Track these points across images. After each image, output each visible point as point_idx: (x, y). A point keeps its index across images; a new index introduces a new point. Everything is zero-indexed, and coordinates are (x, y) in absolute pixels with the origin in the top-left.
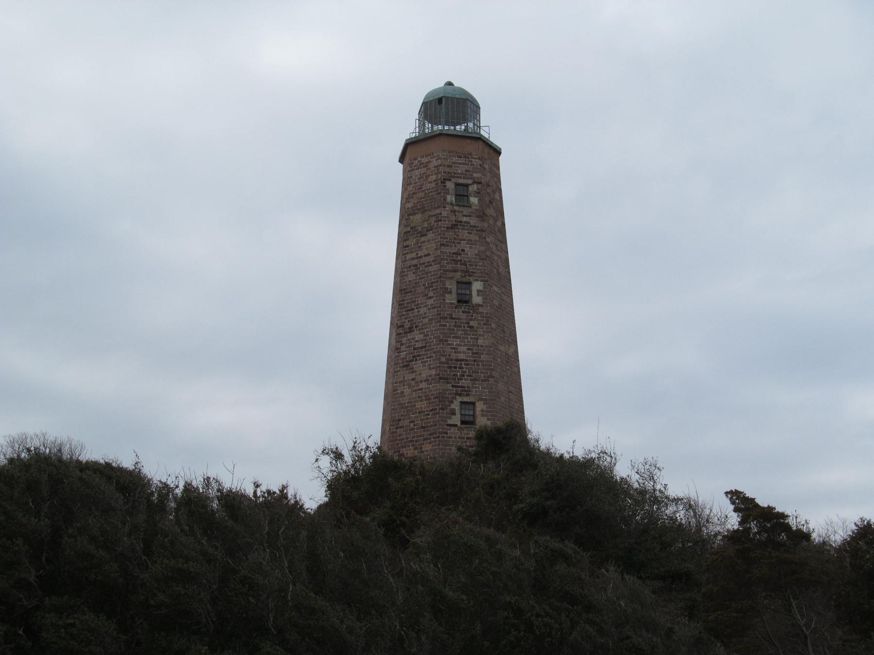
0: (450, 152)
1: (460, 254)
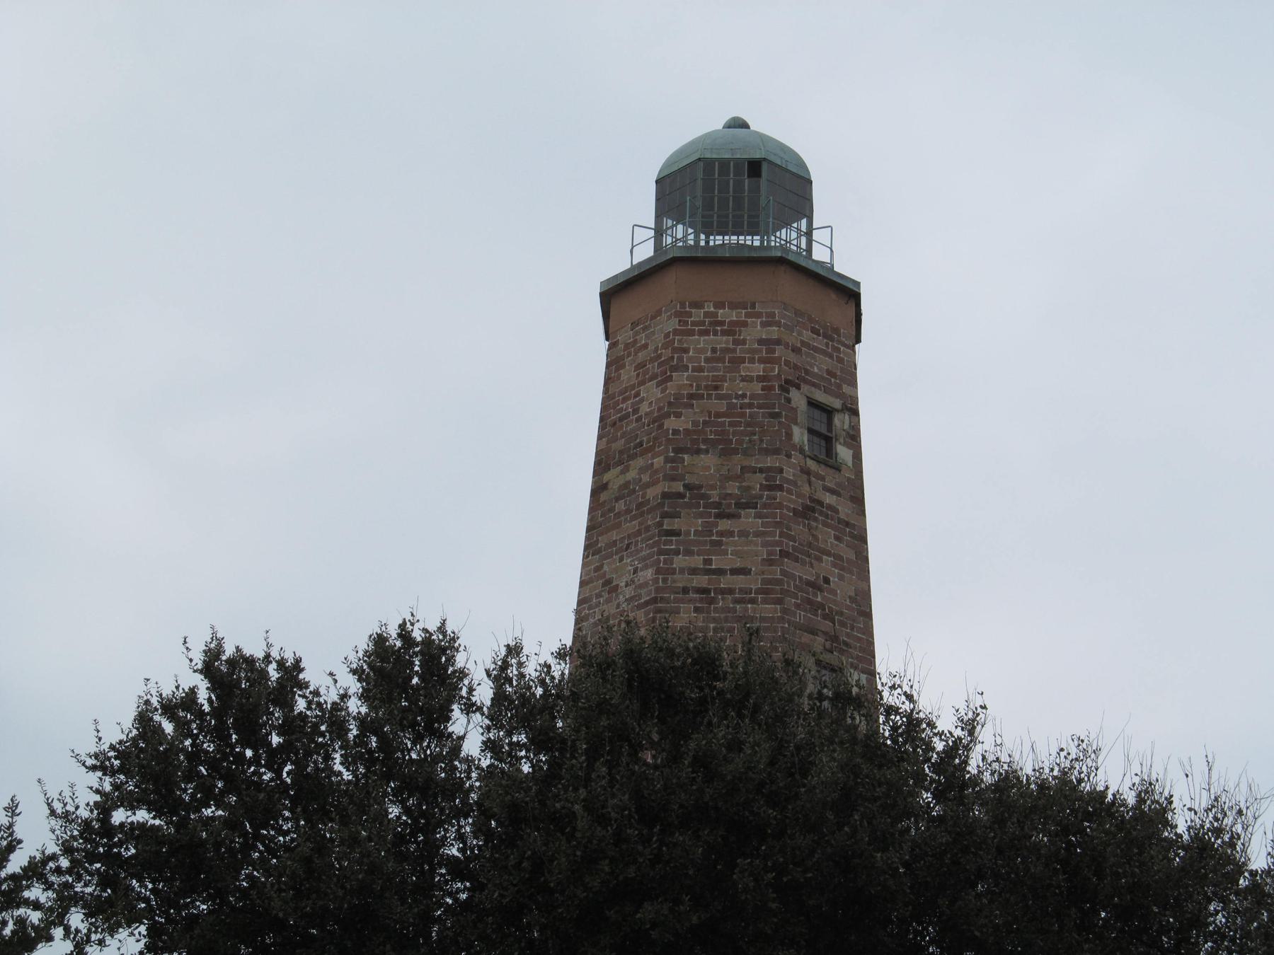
0: (798, 313)
1: (820, 589)
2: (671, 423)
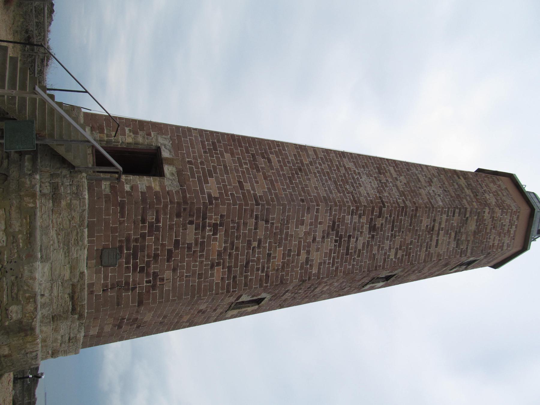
2: (487, 210)
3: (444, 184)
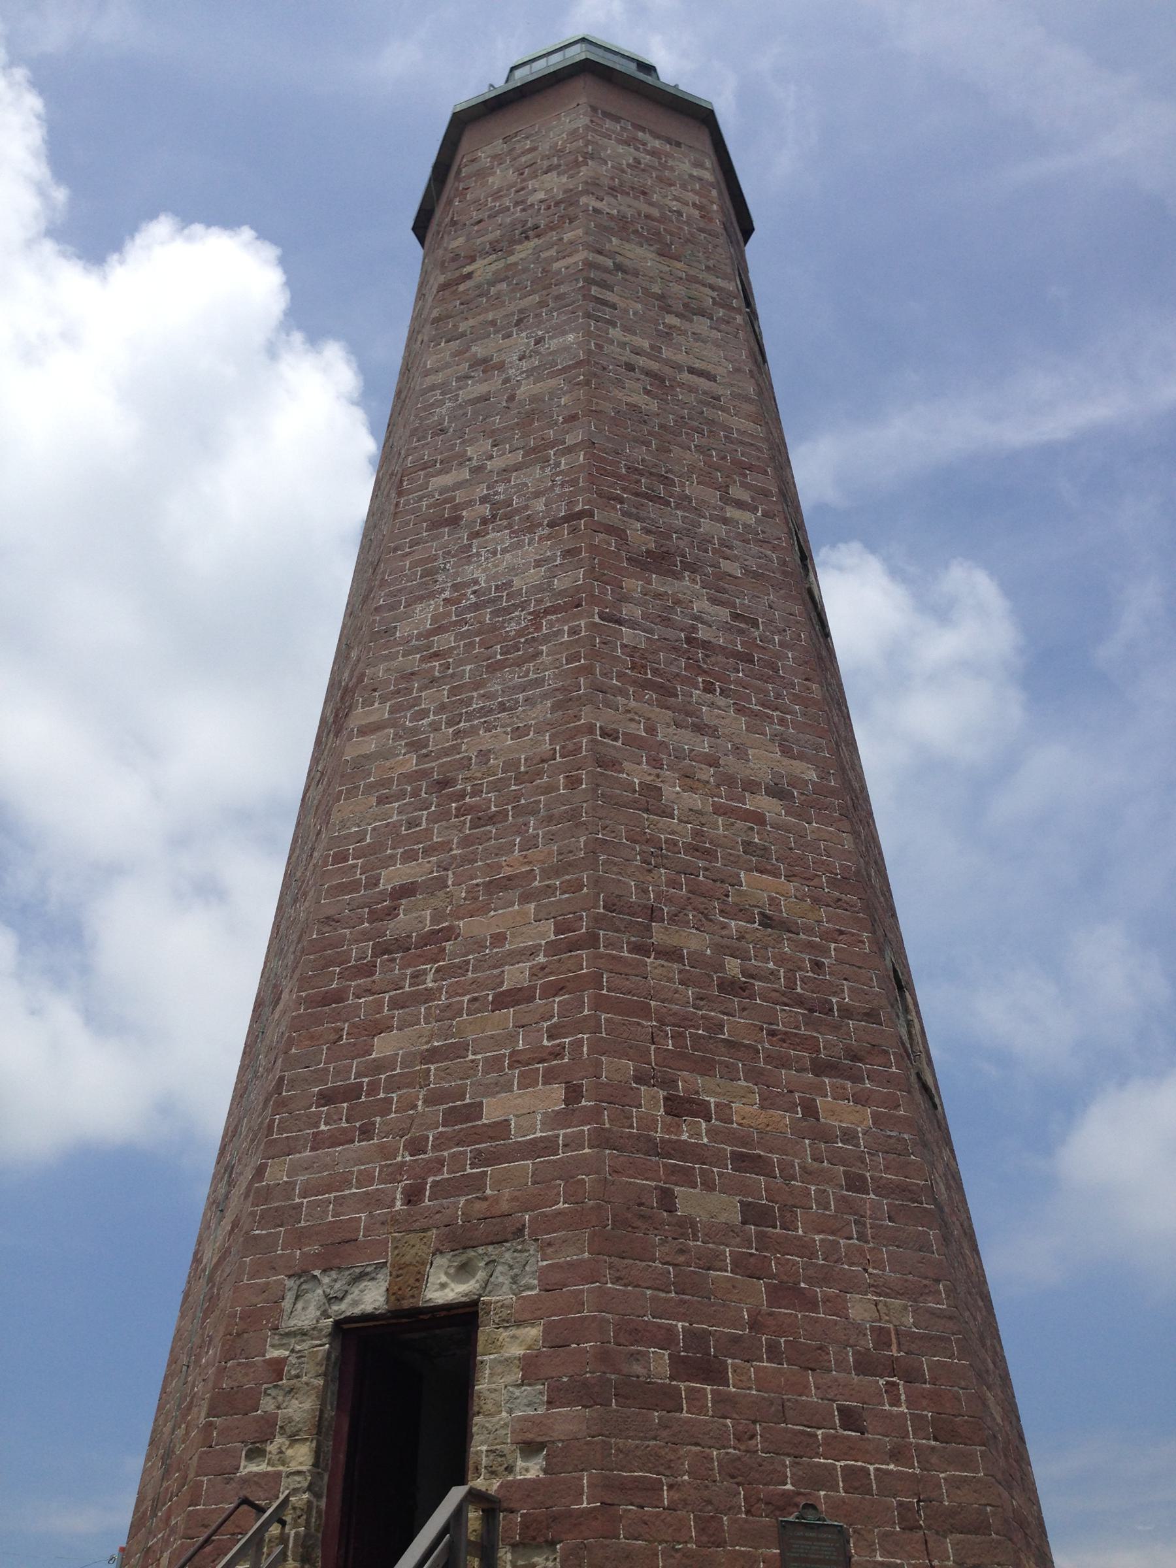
3: (493, 323)
